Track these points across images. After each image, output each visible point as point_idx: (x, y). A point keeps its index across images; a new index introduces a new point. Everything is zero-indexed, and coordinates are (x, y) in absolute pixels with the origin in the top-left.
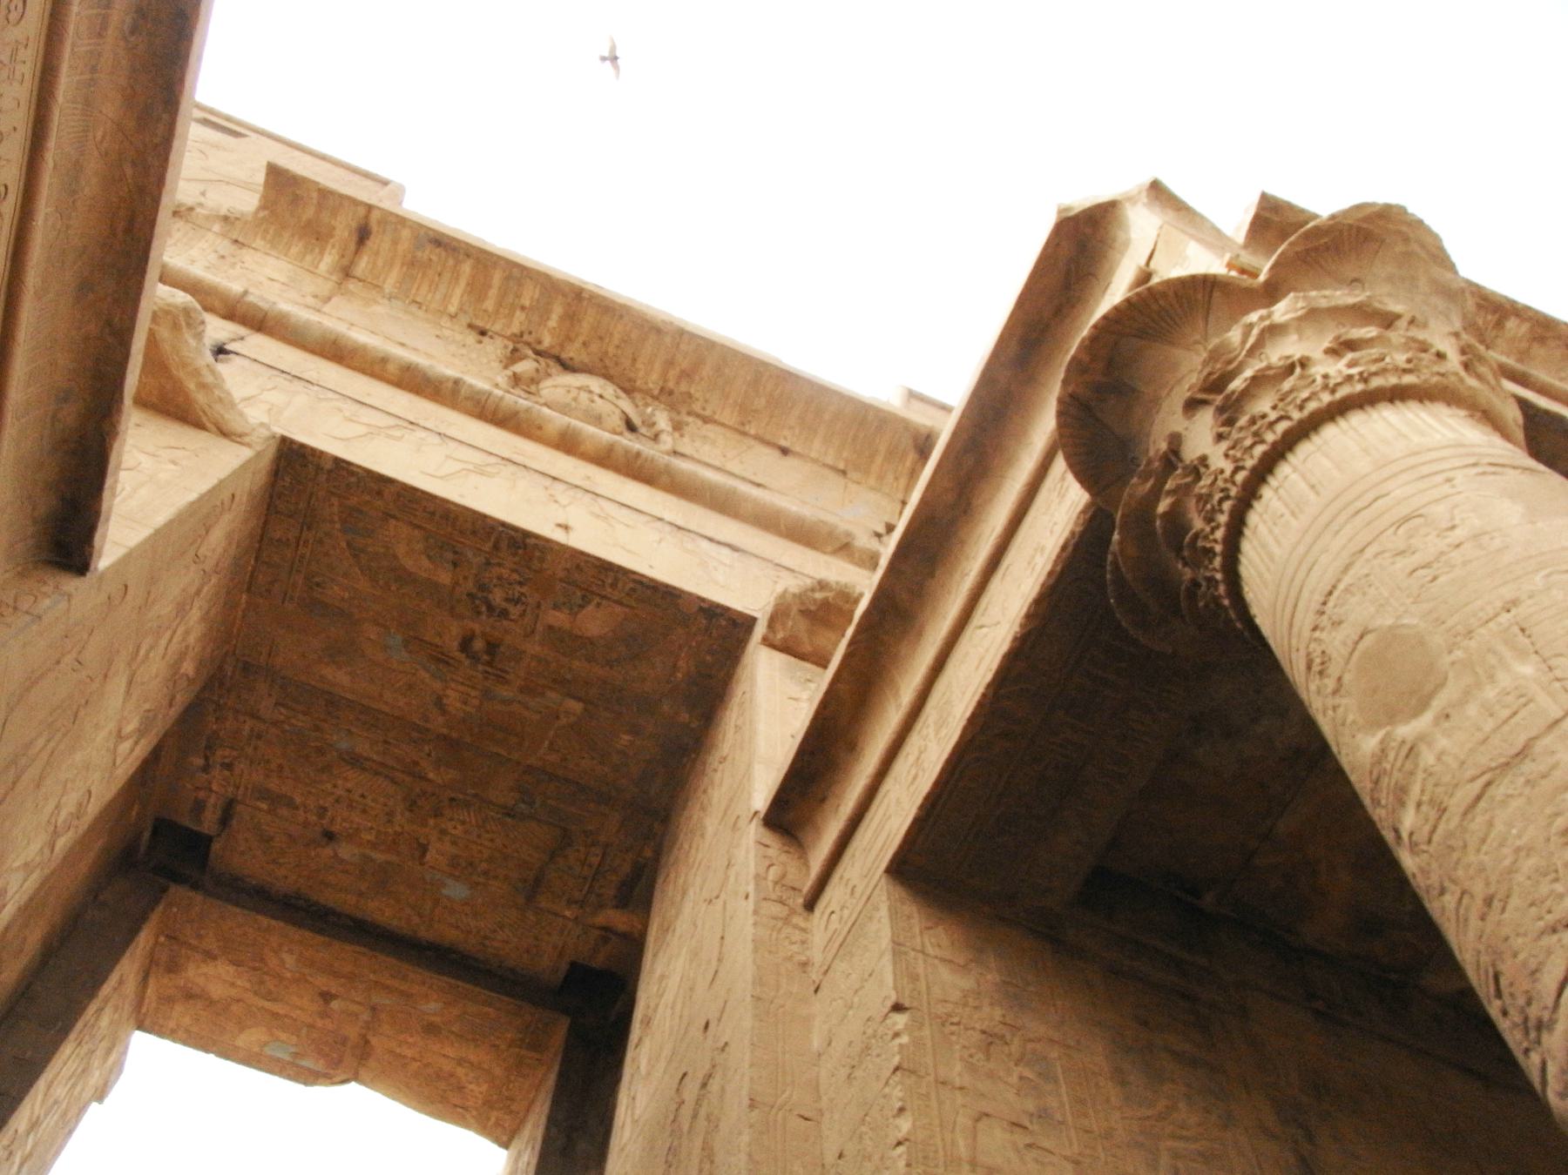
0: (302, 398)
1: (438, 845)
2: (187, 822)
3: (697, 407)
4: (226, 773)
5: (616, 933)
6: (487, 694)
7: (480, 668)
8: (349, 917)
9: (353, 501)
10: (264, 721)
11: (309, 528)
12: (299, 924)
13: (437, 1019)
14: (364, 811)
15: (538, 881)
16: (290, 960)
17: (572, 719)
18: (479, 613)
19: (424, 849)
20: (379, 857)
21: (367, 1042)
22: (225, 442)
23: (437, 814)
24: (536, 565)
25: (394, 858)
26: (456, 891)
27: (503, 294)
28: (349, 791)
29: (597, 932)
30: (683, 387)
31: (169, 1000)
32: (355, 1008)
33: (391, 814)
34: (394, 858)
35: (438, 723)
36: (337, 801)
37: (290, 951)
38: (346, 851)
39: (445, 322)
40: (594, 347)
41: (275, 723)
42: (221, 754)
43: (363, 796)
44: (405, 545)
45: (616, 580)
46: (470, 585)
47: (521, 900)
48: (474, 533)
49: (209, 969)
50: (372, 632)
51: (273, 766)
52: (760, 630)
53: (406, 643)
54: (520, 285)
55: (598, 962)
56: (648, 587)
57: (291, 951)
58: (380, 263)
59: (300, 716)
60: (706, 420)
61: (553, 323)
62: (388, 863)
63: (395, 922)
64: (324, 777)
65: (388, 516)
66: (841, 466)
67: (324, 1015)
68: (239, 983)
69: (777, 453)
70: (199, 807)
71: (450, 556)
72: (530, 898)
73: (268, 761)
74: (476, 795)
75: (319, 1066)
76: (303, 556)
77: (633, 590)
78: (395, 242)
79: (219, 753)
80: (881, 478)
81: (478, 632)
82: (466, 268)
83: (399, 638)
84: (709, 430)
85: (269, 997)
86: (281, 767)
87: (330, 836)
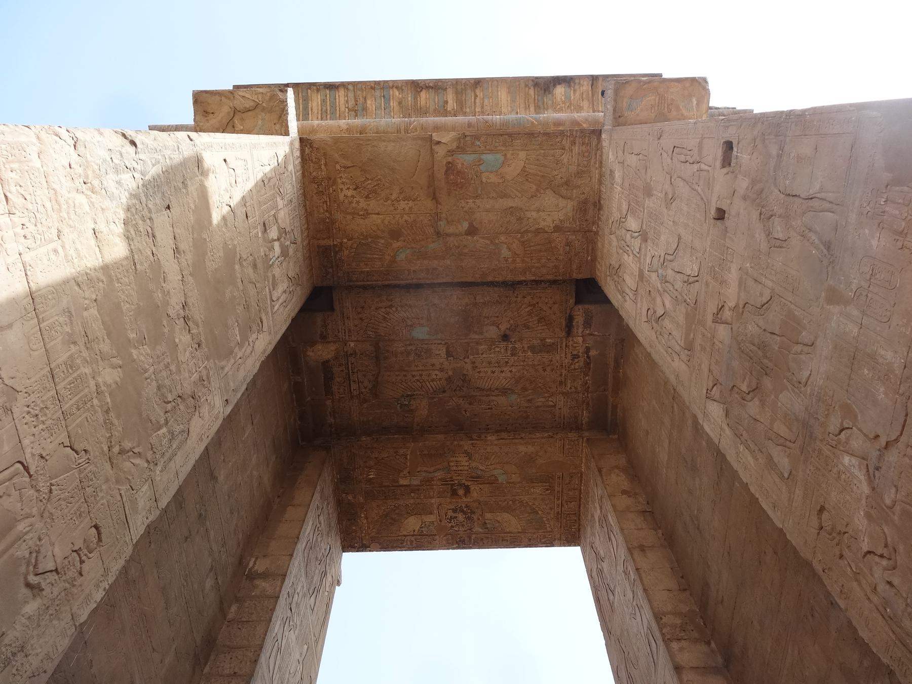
4: (575, 353)
11: (558, 513)
13: (396, 245)
14: (490, 363)
17: (401, 475)
18: (466, 506)
19: (449, 354)
23: (449, 379)
28: (502, 372)
31: (579, 174)
32: (451, 230)
33: (474, 368)
36: (507, 362)
38: (492, 332)
42: (581, 363)
43: (493, 372)
44: (510, 521)
45: (411, 544)
47: (381, 344)
48: (482, 539)
50: (515, 478)
51: (549, 369)
57: (506, 259)
65: (524, 531)
68: (534, 214)
70: (587, 323)
76: (558, 499)
79: (582, 364)
83: (500, 480)
85: (511, 210)
86: (545, 370)
87: (505, 337)
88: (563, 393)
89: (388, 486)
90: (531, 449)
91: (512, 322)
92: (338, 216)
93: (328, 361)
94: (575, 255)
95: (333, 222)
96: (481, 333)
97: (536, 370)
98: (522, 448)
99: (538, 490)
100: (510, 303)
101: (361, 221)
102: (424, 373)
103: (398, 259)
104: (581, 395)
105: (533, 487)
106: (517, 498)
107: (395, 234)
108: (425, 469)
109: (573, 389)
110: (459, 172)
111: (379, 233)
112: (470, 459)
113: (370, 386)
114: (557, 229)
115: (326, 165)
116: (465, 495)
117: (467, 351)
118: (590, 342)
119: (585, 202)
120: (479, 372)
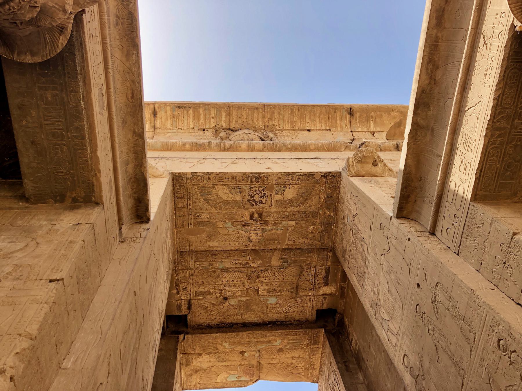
0: (168, 162)
1: (262, 287)
2: (179, 314)
3: (277, 127)
5: (328, 295)
6: (263, 231)
7: (259, 223)
8: (240, 323)
9: (201, 185)
10: (193, 269)
12: (226, 332)
13: (281, 347)
14: (235, 286)
15: (297, 288)
16: (226, 345)
17: (293, 228)
18: (253, 205)
19: (258, 291)
20: (244, 299)
21: (260, 363)
22: (157, 179)
24: (266, 182)
25: (248, 298)
26: (272, 300)
27: (205, 115)
28: (227, 281)
29: (321, 297)
30: (271, 123)
31: (190, 375)
32: (253, 353)
33: (243, 283)
34: (248, 298)
35: (251, 246)
36: (225, 286)
37: (225, 342)
38: (233, 302)
39: (191, 131)
40: (239, 122)
41: (197, 269)
42: (181, 286)
43: (232, 281)
44: (223, 193)
45: (293, 177)
46: (247, 197)
47: (295, 295)
48: (243, 180)
49: (200, 359)
50: (220, 225)
51: (200, 283)
52: (344, 174)
53: (232, 224)
54: (210, 111)
55: (325, 307)
56: (303, 176)
57: (226, 342)
58: (163, 120)
59: (204, 263)
60: (282, 131)
61: (224, 119)
62: (247, 300)
63: (256, 319)
64: (218, 279)
65: (214, 185)
66: (328, 128)
67: (243, 360)
68: (212, 360)
69: (307, 132)
70: (179, 307)
71: (238, 190)
72: (297, 293)
73: (198, 282)
74: (268, 266)
75: (247, 378)
77: (299, 178)
78: (166, 112)
80: (341, 127)
81: (254, 211)
82: (191, 112)
84: (285, 133)
87: (226, 299)
88: (191, 269)
89: (302, 220)
90: (210, 244)
91: (222, 307)
92: (306, 357)
93: (325, 286)
94: (190, 345)
95: (309, 355)
96: (239, 301)
97: (207, 282)
98: (216, 244)
99: (205, 217)
100: (223, 315)
101: (296, 355)
102: (272, 280)
103: (280, 341)
104: (180, 268)
105: (208, 218)
106: (219, 211)
107: (280, 350)
108: (278, 232)
109: (185, 271)
110: (248, 374)
111: (288, 351)
112: (249, 238)
113: (304, 273)
114: (200, 355)
115: (308, 375)
116: (253, 213)
117: (247, 292)
118: (177, 296)
119: (187, 365)
120: (241, 281)
